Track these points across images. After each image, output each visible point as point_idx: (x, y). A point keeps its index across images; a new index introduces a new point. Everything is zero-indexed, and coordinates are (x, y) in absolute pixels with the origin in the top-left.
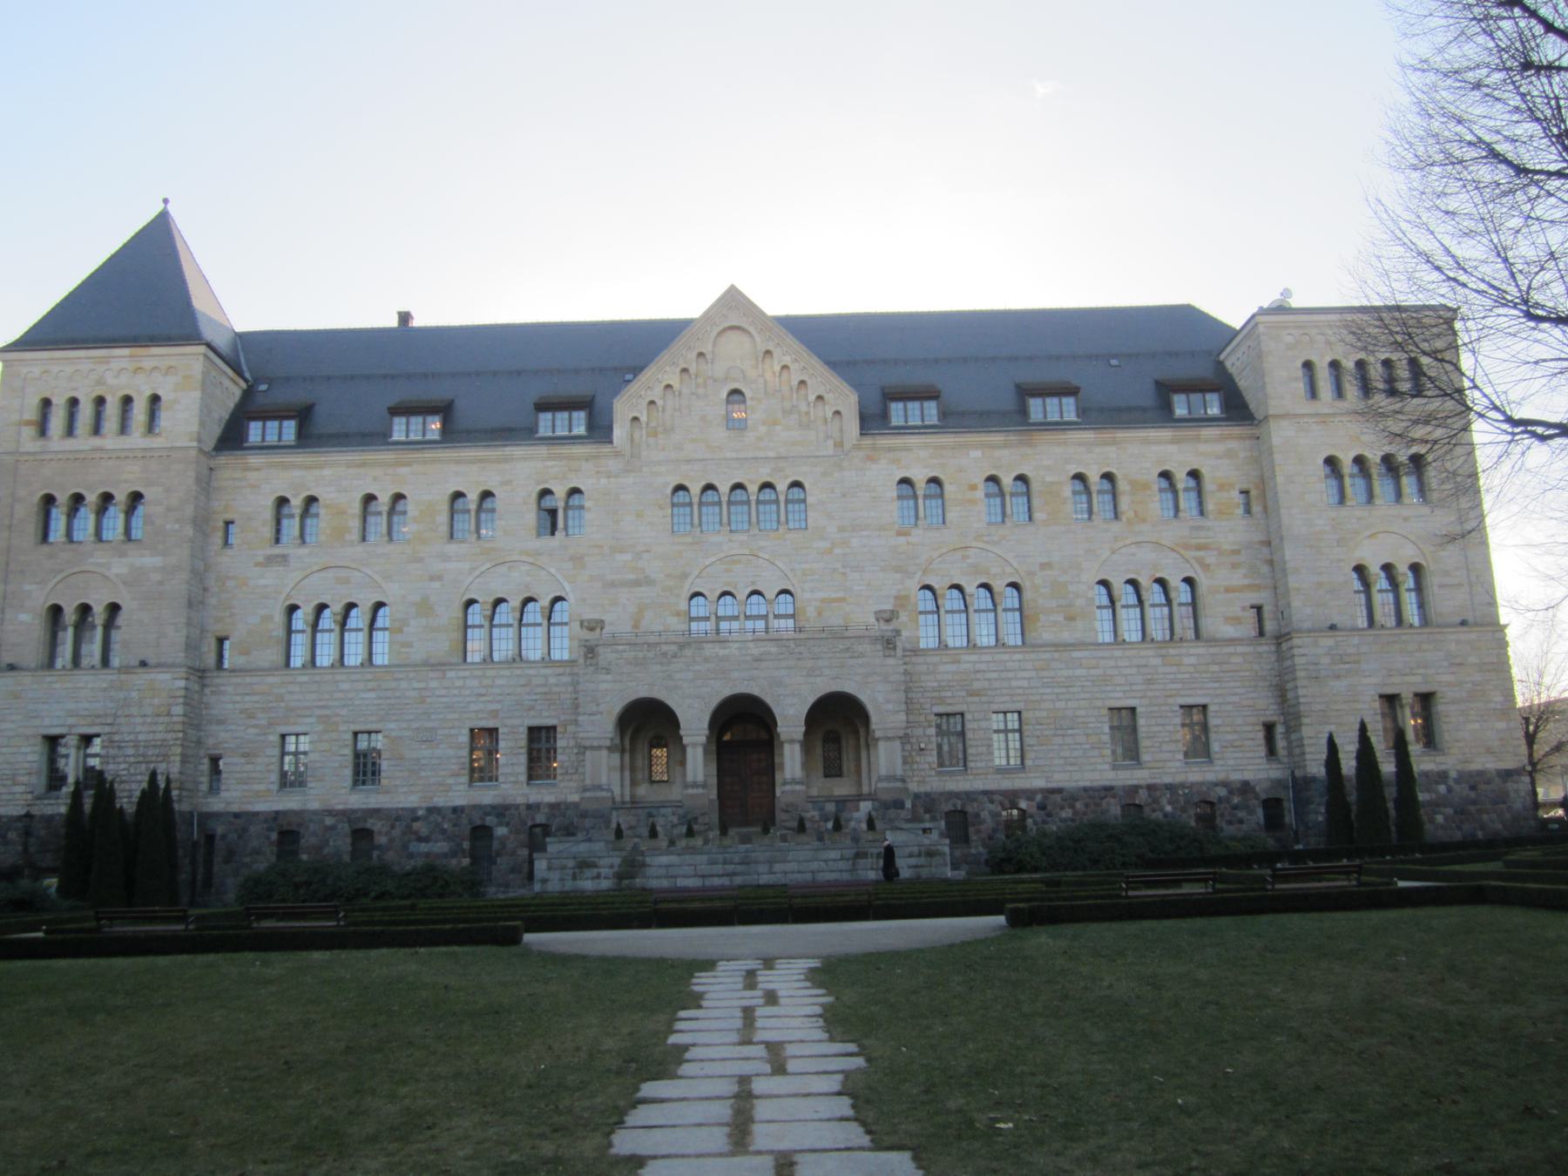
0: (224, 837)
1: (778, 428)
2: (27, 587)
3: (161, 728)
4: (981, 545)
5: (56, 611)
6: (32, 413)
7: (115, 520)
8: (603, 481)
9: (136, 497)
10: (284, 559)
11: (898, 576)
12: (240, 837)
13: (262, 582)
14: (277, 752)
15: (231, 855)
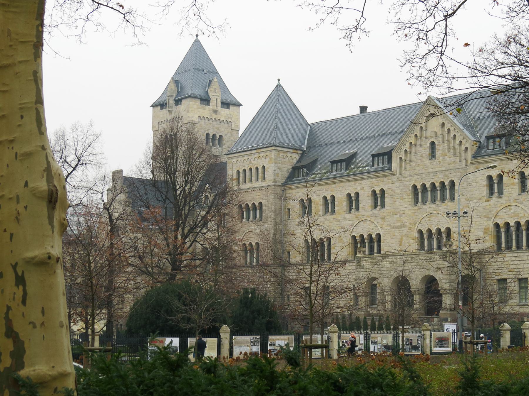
1: (446, 157)
4: (515, 204)
8: (390, 185)
9: (261, 203)
11: (485, 219)
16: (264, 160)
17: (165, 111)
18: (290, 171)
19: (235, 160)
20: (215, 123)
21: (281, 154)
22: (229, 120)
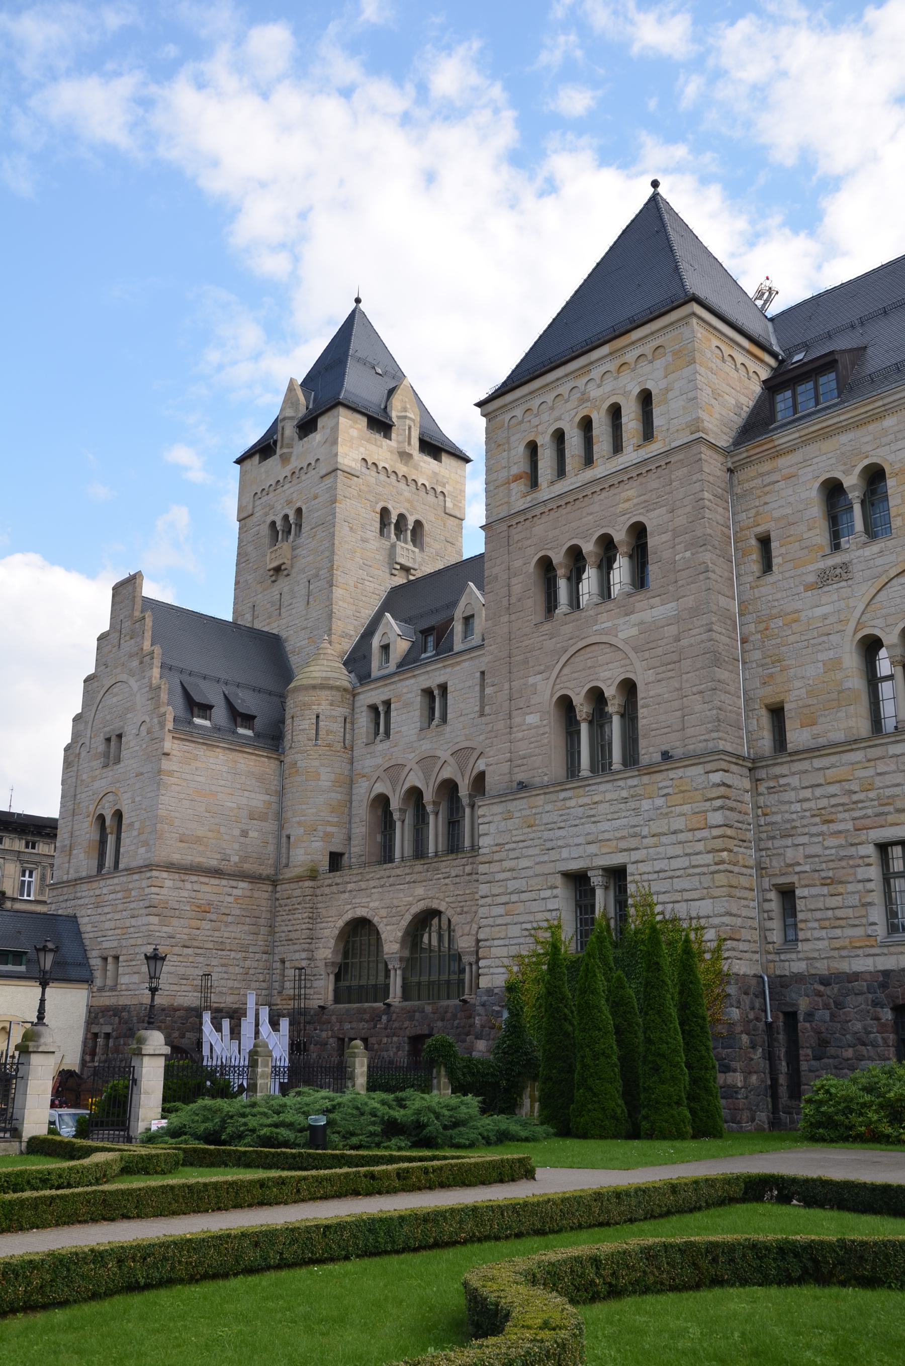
0: (809, 1016)
2: (531, 680)
3: (700, 846)
5: (566, 704)
6: (520, 465)
7: (621, 572)
9: (639, 532)
10: (845, 566)
12: (833, 1016)
13: (819, 611)
14: (874, 872)
15: (823, 1043)
16: (645, 368)
17: (273, 462)
18: (744, 415)
19: (518, 412)
20: (402, 485)
21: (715, 342)
22: (439, 489)
